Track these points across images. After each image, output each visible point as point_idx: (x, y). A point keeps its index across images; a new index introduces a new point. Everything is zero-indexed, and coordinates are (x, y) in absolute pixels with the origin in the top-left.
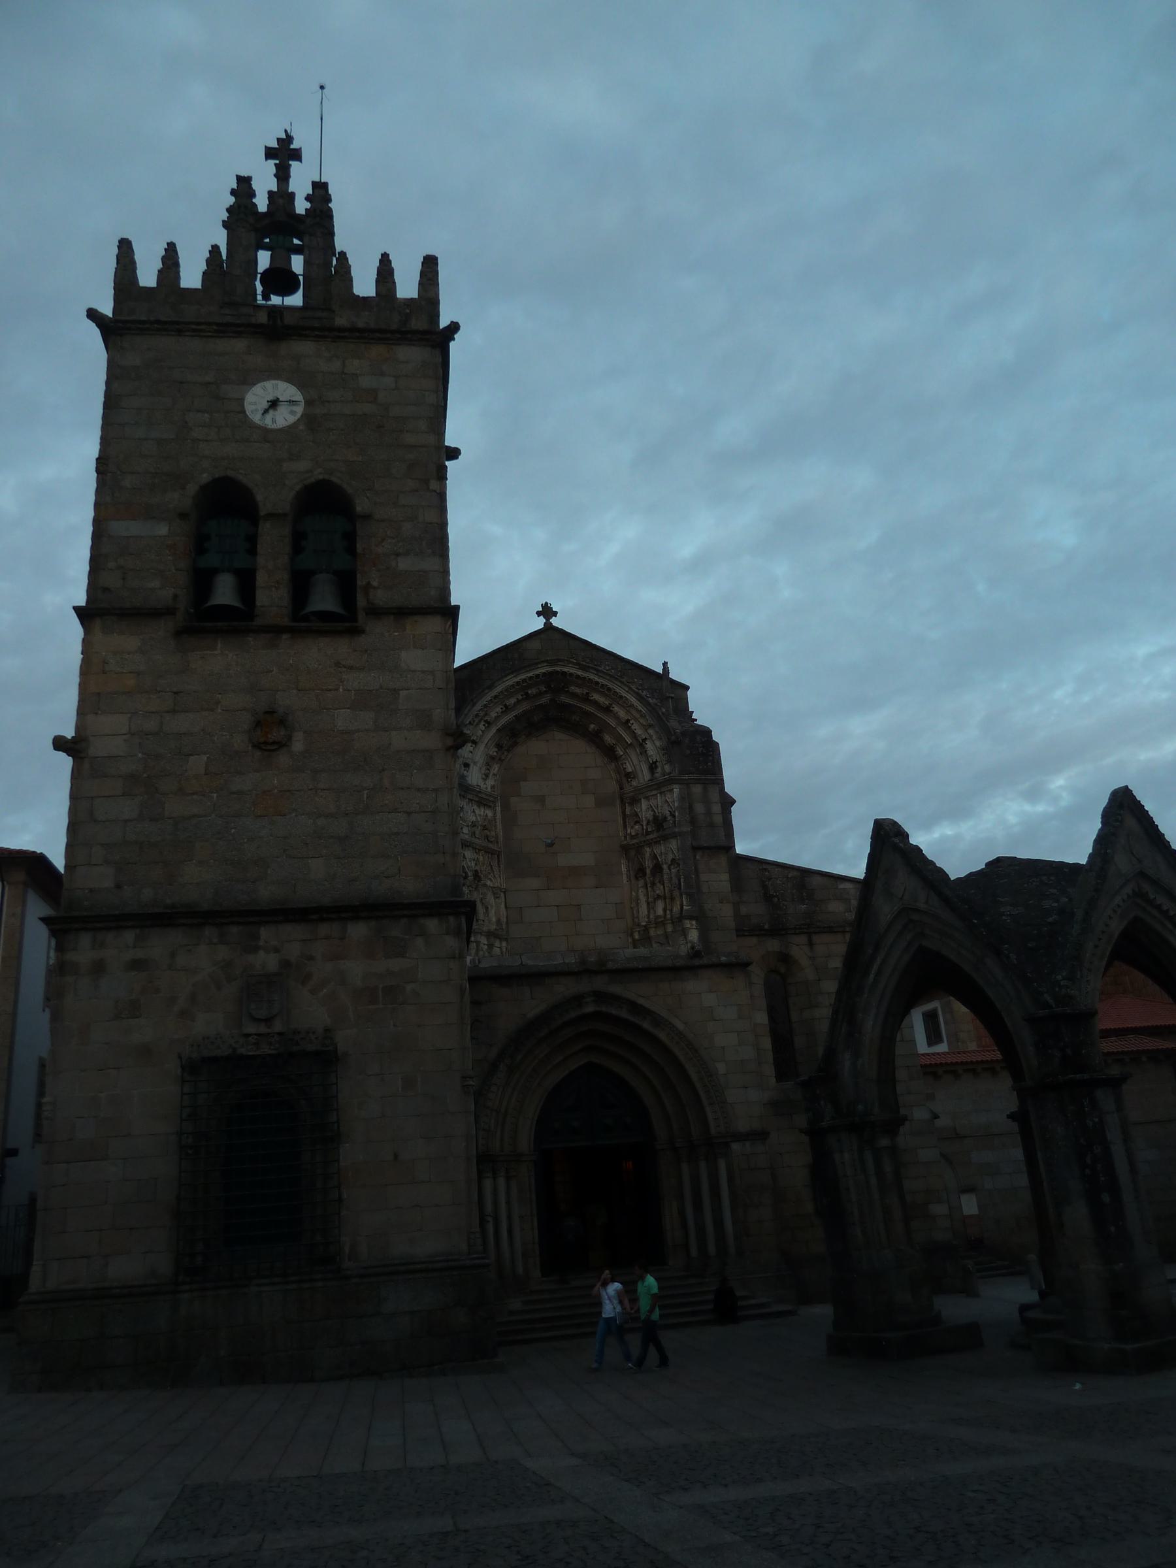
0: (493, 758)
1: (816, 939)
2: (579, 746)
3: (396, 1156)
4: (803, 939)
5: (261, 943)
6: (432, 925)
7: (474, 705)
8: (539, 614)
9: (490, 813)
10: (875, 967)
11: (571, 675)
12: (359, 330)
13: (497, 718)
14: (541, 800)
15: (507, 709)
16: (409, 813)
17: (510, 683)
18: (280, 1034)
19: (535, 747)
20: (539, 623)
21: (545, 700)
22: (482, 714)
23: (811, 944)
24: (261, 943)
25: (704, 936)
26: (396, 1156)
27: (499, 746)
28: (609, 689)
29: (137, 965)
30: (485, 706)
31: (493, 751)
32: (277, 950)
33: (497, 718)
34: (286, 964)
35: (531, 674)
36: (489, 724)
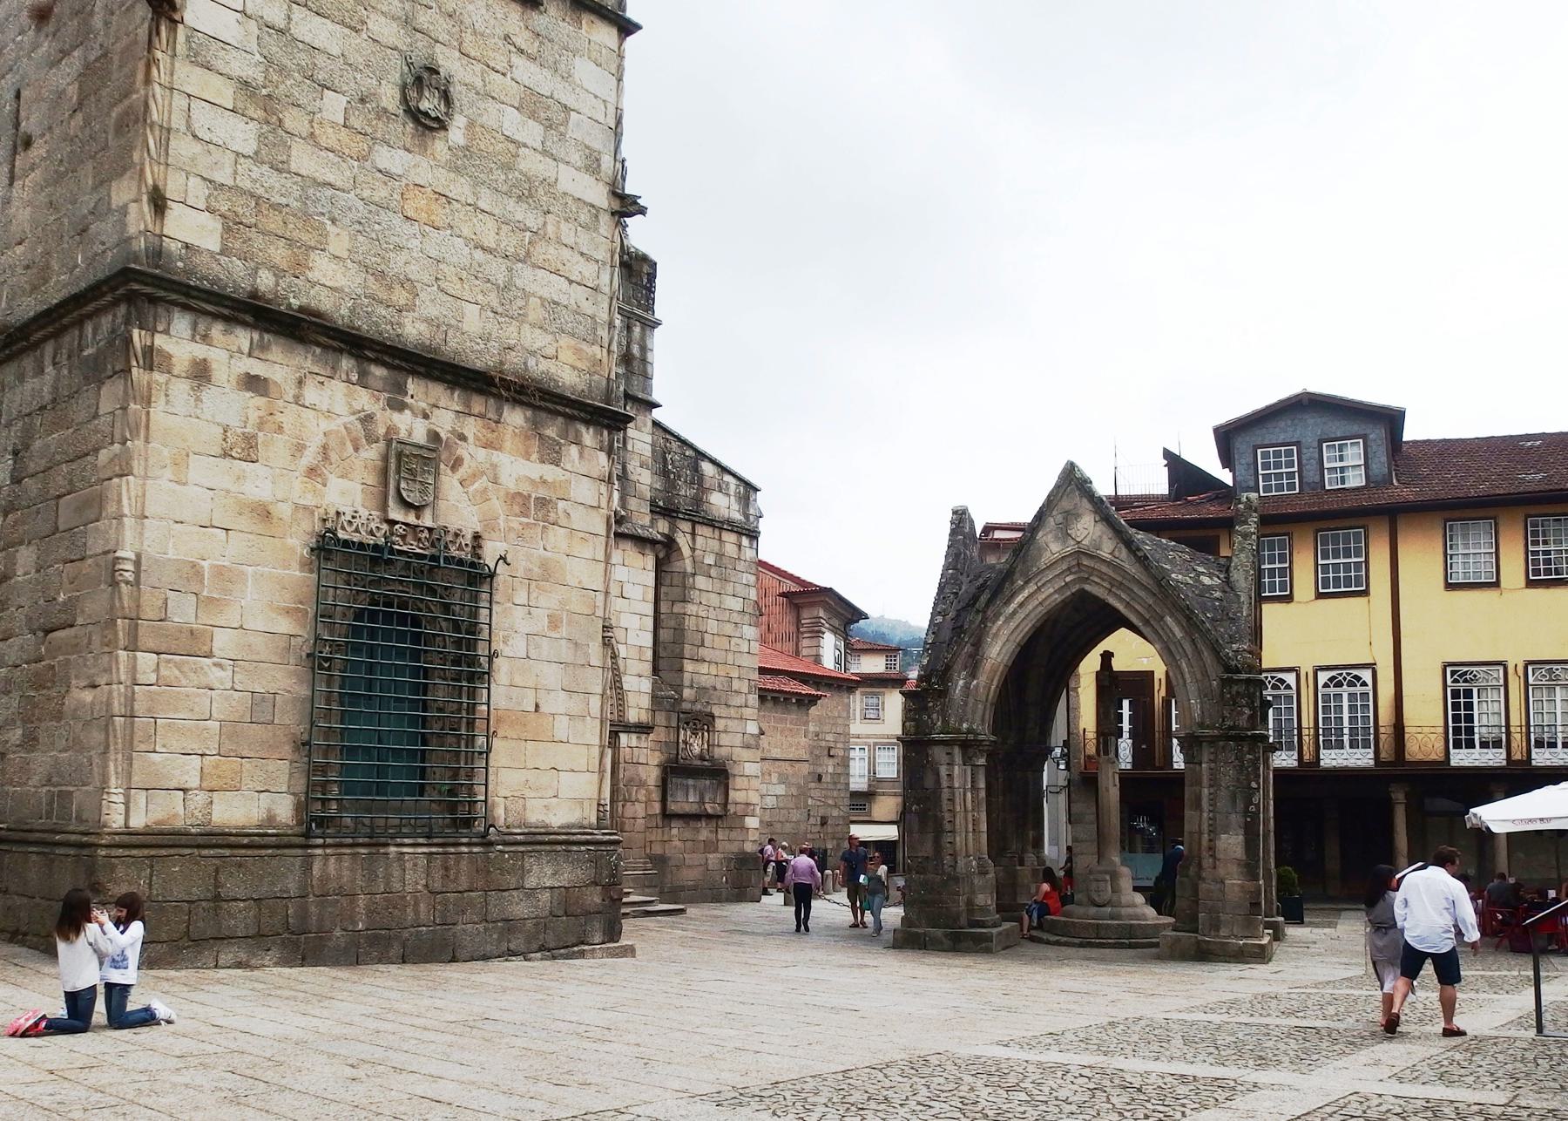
1: (700, 530)
3: (537, 706)
4: (686, 526)
6: (588, 436)
10: (1020, 598)
16: (571, 282)
18: (430, 530)
23: (693, 534)
24: (408, 400)
25: (623, 501)
26: (537, 706)
32: (426, 416)
34: (434, 436)
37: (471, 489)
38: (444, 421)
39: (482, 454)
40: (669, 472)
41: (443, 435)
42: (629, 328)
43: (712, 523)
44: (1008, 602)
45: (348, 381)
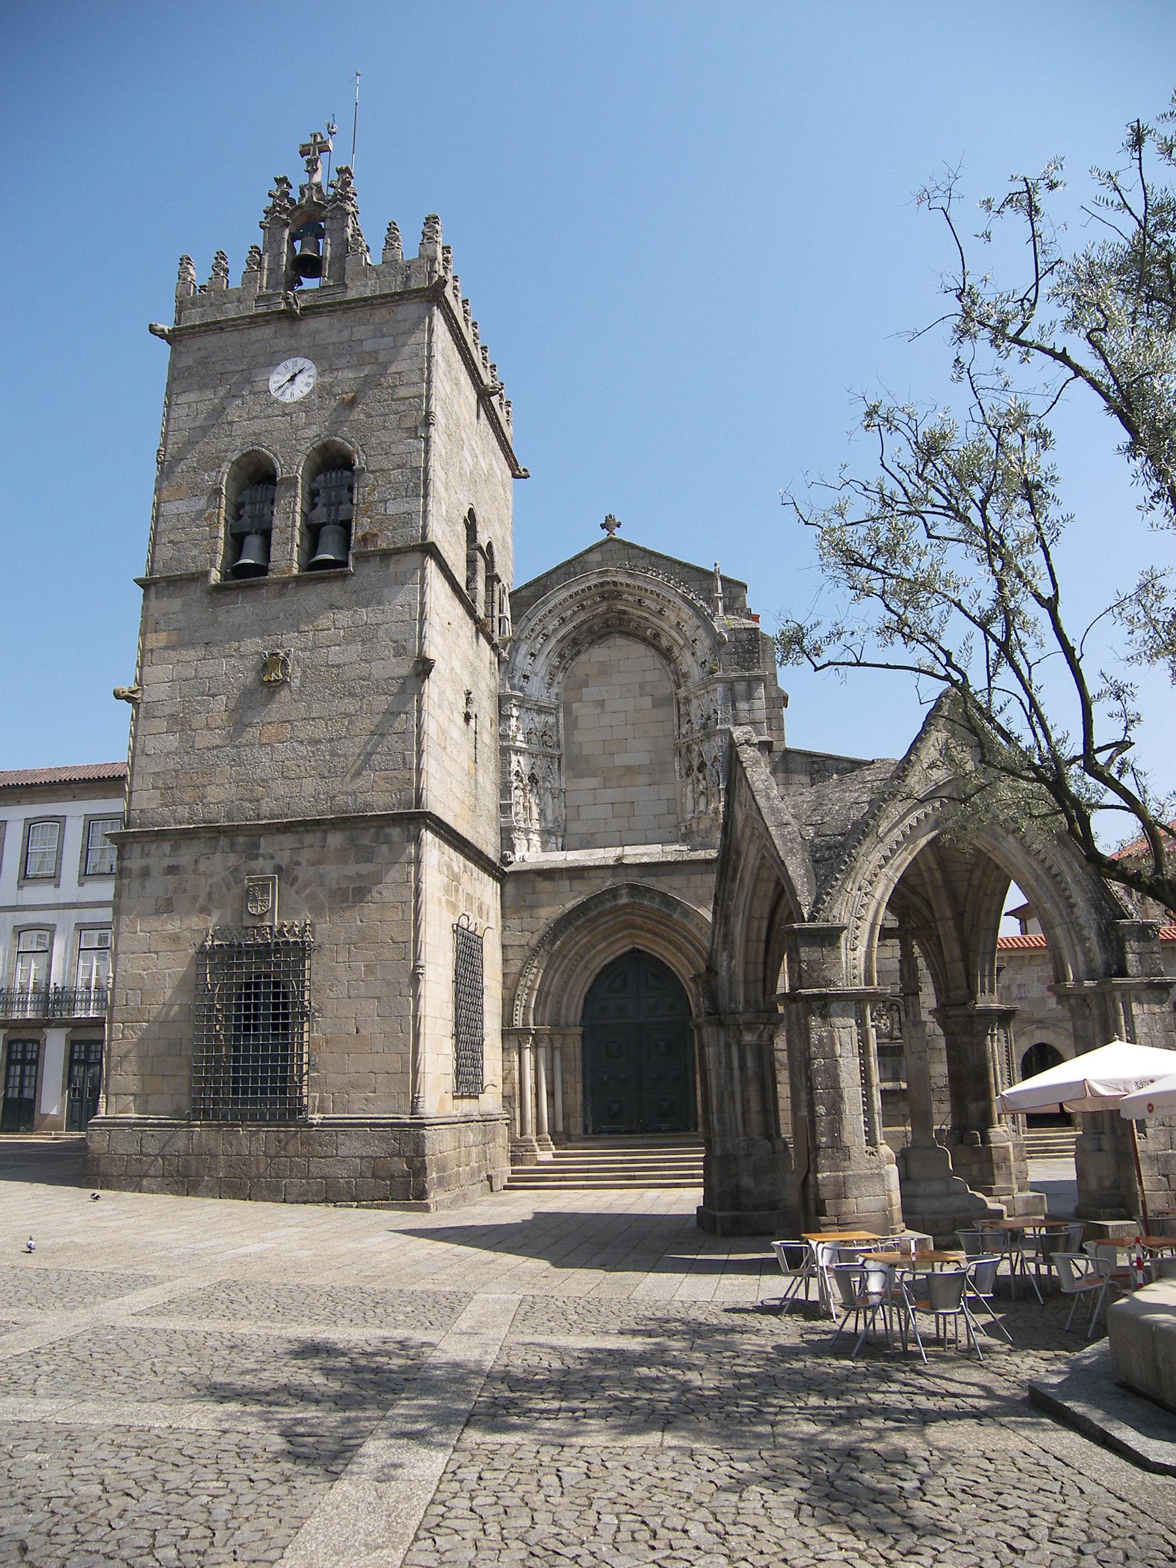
0: (557, 668)
2: (640, 649)
5: (261, 851)
8: (603, 526)
9: (551, 720)
11: (621, 584)
12: (366, 299)
14: (602, 703)
17: (563, 596)
19: (597, 654)
20: (603, 535)
21: (601, 609)
22: (538, 628)
27: (561, 656)
28: (658, 595)
29: (172, 870)
30: (541, 621)
31: (556, 661)
32: (272, 858)
33: (555, 630)
36: (547, 637)
37: (304, 894)
38: (284, 859)
39: (312, 870)
41: (284, 867)
42: (731, 689)
44: (733, 879)
45: (224, 852)
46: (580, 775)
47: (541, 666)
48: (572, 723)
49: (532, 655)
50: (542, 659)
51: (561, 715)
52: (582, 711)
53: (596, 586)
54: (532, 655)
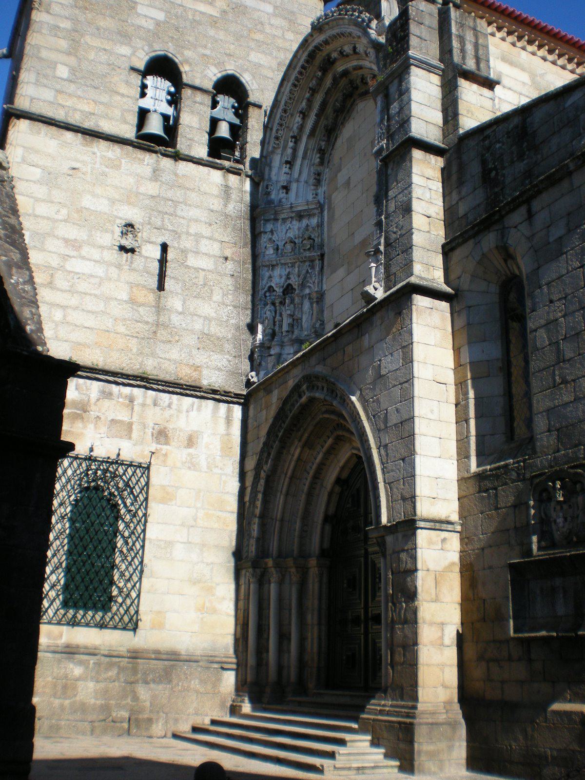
1: (536, 205)
7: (271, 129)
9: (314, 221)
13: (301, 128)
14: (348, 183)
15: (304, 115)
19: (347, 131)
21: (328, 82)
23: (530, 215)
27: (322, 152)
33: (301, 128)
35: (298, 69)
36: (296, 139)
40: (491, 170)
43: (553, 181)
46: (334, 271)
47: (303, 170)
48: (332, 218)
49: (287, 162)
50: (299, 162)
51: (326, 213)
52: (338, 198)
53: (307, 61)
54: (287, 162)
